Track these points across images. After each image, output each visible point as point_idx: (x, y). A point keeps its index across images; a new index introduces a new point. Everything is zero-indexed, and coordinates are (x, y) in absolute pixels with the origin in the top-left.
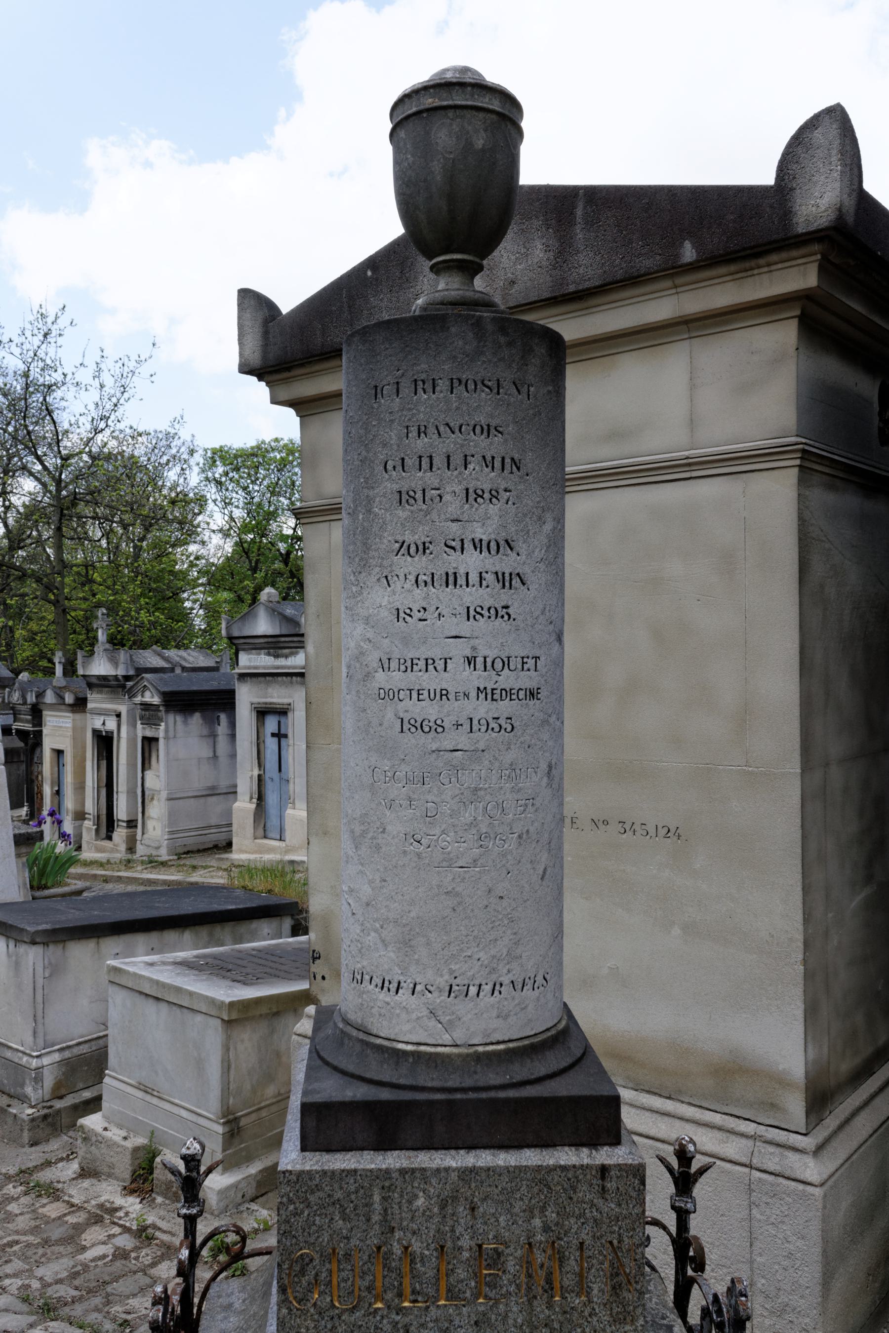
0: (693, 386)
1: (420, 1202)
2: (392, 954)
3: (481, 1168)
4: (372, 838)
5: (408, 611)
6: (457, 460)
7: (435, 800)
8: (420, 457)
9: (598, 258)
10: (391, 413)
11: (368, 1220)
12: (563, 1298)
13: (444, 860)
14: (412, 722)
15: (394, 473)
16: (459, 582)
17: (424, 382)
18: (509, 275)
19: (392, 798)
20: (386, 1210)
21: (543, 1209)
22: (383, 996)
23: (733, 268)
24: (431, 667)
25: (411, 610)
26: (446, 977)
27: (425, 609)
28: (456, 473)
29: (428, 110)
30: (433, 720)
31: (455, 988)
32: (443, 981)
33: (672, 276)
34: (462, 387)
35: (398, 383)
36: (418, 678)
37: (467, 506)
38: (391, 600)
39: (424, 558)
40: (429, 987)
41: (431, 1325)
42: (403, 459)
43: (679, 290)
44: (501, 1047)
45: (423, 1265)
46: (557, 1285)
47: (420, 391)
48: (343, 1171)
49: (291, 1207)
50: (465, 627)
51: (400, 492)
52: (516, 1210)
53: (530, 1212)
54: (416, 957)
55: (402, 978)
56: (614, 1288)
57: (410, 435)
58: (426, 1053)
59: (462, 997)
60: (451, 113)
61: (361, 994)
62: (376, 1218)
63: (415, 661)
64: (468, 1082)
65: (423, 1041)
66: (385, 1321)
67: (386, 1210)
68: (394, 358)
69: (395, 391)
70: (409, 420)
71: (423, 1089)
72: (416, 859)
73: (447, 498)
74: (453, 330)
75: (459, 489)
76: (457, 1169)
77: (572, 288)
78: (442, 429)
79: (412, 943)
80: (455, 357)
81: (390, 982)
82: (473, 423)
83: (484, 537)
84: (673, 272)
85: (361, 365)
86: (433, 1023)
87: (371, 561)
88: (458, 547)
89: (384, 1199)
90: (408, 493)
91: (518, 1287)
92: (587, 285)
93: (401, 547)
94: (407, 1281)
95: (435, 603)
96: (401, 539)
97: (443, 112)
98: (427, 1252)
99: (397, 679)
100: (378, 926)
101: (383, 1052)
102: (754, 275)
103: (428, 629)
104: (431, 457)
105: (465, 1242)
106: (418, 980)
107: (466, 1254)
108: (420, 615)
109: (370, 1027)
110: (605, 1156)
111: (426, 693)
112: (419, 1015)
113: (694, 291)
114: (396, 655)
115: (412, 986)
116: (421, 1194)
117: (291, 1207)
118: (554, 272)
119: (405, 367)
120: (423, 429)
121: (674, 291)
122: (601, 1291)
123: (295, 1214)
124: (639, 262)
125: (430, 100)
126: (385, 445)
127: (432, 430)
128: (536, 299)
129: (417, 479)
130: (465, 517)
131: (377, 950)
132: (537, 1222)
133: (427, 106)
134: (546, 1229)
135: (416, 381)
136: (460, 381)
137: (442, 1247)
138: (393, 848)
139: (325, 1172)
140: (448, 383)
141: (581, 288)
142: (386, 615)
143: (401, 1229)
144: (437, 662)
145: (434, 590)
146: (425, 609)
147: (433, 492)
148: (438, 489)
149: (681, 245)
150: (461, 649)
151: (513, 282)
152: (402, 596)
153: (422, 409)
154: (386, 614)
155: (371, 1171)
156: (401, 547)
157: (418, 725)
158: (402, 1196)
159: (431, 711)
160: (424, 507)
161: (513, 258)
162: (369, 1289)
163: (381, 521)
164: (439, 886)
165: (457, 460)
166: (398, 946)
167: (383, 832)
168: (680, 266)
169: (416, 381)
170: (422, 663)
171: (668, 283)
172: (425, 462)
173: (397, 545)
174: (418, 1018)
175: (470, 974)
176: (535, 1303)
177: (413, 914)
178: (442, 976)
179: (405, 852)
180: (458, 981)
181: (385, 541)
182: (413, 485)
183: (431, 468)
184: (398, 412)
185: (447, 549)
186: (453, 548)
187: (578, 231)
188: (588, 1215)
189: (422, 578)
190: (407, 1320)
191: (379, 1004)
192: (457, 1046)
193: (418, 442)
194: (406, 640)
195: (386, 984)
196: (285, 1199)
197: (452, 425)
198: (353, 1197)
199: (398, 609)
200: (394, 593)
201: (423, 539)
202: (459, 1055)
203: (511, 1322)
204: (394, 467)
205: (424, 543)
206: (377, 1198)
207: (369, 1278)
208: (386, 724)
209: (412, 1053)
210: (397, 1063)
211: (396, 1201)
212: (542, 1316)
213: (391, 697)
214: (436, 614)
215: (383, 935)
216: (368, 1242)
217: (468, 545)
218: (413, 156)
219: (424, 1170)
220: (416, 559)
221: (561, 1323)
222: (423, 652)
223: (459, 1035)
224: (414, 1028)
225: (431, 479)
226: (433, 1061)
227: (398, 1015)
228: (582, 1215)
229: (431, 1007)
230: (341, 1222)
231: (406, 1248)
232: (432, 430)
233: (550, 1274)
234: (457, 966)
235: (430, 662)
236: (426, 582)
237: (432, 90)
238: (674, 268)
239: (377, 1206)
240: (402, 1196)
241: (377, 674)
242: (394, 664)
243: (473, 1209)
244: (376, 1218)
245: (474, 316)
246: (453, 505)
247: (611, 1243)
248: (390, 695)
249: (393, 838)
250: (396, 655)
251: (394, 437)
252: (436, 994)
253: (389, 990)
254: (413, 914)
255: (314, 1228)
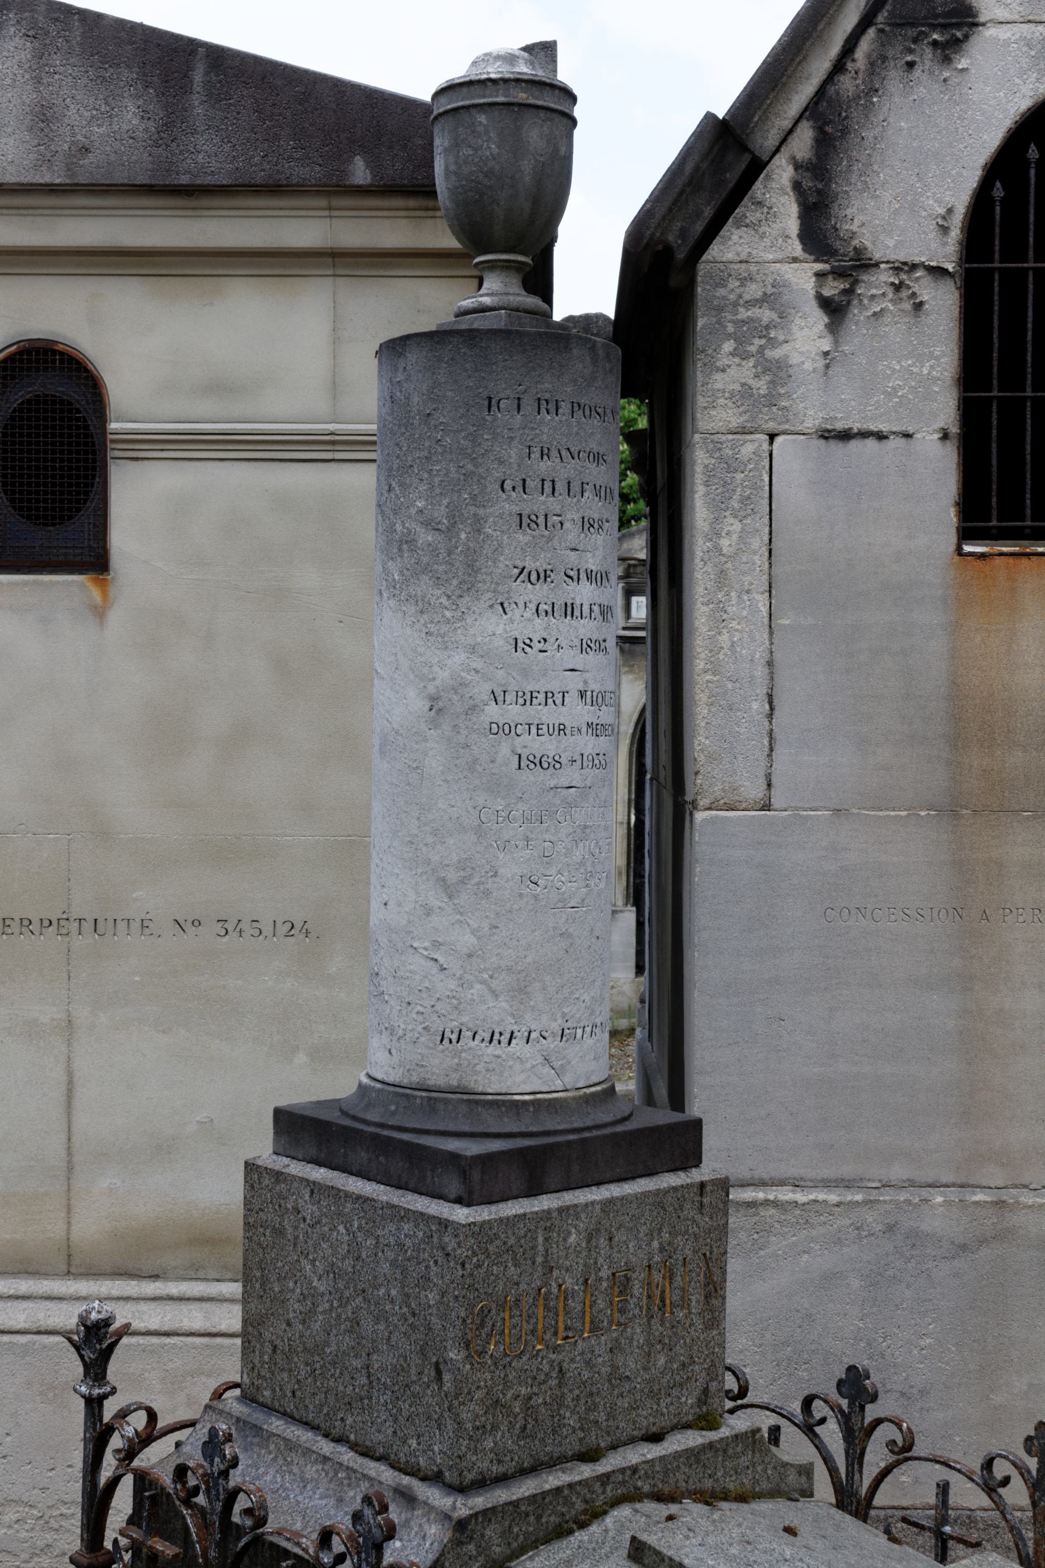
0: (336, 341)
1: (573, 1239)
2: (504, 1004)
3: (617, 1198)
4: (478, 884)
5: (528, 642)
6: (576, 487)
7: (553, 839)
8: (543, 480)
9: (227, 148)
10: (510, 429)
11: (533, 1263)
12: (672, 1313)
13: (559, 901)
14: (531, 758)
15: (514, 494)
16: (575, 614)
17: (547, 402)
18: (79, 137)
19: (506, 839)
20: (547, 1251)
21: (660, 1230)
22: (492, 1050)
23: (412, 203)
24: (550, 701)
25: (531, 640)
26: (560, 1021)
27: (545, 640)
28: (575, 500)
29: (520, 105)
30: (551, 756)
31: (566, 1031)
32: (556, 1026)
33: (329, 194)
34: (581, 411)
35: (519, 399)
36: (537, 712)
37: (583, 535)
38: (508, 629)
39: (545, 587)
40: (544, 1034)
41: (578, 1358)
42: (524, 481)
43: (334, 213)
44: (598, 1088)
45: (574, 1301)
46: (668, 1302)
47: (543, 411)
48: (515, 1216)
49: (475, 1260)
50: (579, 660)
51: (520, 515)
52: (641, 1235)
53: (650, 1234)
54: (532, 1003)
55: (515, 1028)
56: (706, 1297)
57: (532, 456)
58: (545, 1100)
59: (571, 1040)
60: (542, 114)
61: (457, 1054)
62: (539, 1260)
63: (534, 695)
64: (589, 1123)
65: (537, 1090)
66: (544, 1362)
67: (547, 1251)
68: (514, 372)
69: (515, 406)
70: (532, 440)
71: (556, 1133)
72: (533, 901)
73: (567, 525)
74: (575, 351)
75: (577, 517)
76: (600, 1202)
77: (184, 179)
78: (564, 453)
79: (528, 989)
80: (576, 380)
81: (501, 1034)
82: (588, 450)
83: (594, 568)
84: (335, 191)
85: (466, 370)
86: (547, 1069)
87: (480, 585)
88: (575, 578)
89: (546, 1239)
90: (529, 517)
91: (641, 1308)
92: (209, 180)
93: (521, 573)
94: (561, 1319)
95: (555, 633)
96: (521, 565)
97: (535, 111)
98: (576, 1288)
99: (514, 712)
100: (486, 976)
101: (499, 1107)
102: (435, 217)
103: (549, 661)
104: (553, 481)
105: (605, 1273)
106: (533, 1028)
107: (605, 1284)
108: (541, 646)
109: (472, 1085)
110: (696, 1176)
111: (545, 727)
112: (534, 1063)
113: (354, 220)
114: (513, 687)
115: (526, 1034)
116: (574, 1230)
117: (475, 1260)
118: (157, 151)
119: (527, 384)
120: (546, 451)
121: (326, 213)
122: (698, 1301)
123: (478, 1266)
124: (290, 167)
125: (524, 95)
126: (501, 462)
127: (554, 453)
128: (126, 181)
129: (540, 503)
130: (581, 547)
131: (484, 1002)
132: (655, 1244)
133: (521, 101)
134: (662, 1249)
135: (539, 399)
136: (579, 405)
137: (586, 1280)
138: (507, 892)
139: (501, 1219)
140: (570, 406)
141: (199, 182)
142: (501, 644)
143: (558, 1268)
144: (556, 695)
145: (554, 621)
146: (545, 640)
147: (555, 518)
148: (559, 516)
149: (350, 160)
150: (574, 683)
151: (86, 150)
152: (520, 625)
153: (546, 431)
154: (501, 643)
155: (536, 1213)
156: (521, 573)
157: (537, 761)
158: (559, 1235)
159: (548, 746)
160: (546, 533)
161: (87, 114)
162: (533, 1332)
163: (495, 543)
164: (555, 928)
165: (576, 487)
166: (511, 993)
167: (495, 875)
168: (345, 186)
169: (539, 399)
170: (541, 697)
171: (323, 202)
172: (548, 486)
173: (516, 571)
174: (533, 1067)
175: (578, 1016)
176: (653, 1322)
177: (529, 959)
178: (555, 1020)
179: (521, 895)
180: (569, 1024)
181: (501, 565)
182: (535, 508)
183: (553, 493)
184: (519, 429)
185: (566, 579)
186: (571, 578)
187: (196, 103)
188: (691, 1231)
189: (543, 607)
190: (561, 1357)
191: (486, 1059)
192: (566, 1090)
193: (541, 464)
194: (525, 672)
195: (496, 1036)
196: (470, 1252)
197: (572, 450)
198: (523, 1241)
199: (516, 639)
200: (512, 621)
201: (545, 566)
202: (574, 1098)
203: (635, 1343)
204: (514, 488)
205: (545, 571)
206: (540, 1240)
207: (533, 1321)
208: (499, 760)
209: (532, 1102)
210: (518, 1114)
211: (555, 1240)
212: (657, 1333)
213: (507, 732)
214: (556, 646)
215: (493, 986)
216: (533, 1285)
217: (583, 576)
218: (498, 147)
219: (576, 1206)
220: (538, 586)
221: (670, 1337)
222: (543, 685)
223: (569, 1080)
224: (529, 1077)
225: (553, 504)
226: (552, 1106)
227: (511, 1067)
228: (686, 1232)
229: (545, 1053)
230: (513, 1268)
231: (560, 1286)
232: (554, 453)
233: (663, 1292)
234: (569, 1009)
235: (520, 694)
236: (546, 612)
237: (523, 84)
238: (338, 186)
239: (541, 1248)
240: (559, 1235)
241: (487, 708)
242: (510, 697)
243: (610, 1239)
244: (539, 1260)
245: (590, 340)
246: (572, 533)
247: (704, 1255)
248: (507, 730)
249: (507, 881)
250: (513, 687)
251: (513, 455)
252: (550, 1040)
253: (499, 1042)
254: (529, 959)
255: (492, 1278)
